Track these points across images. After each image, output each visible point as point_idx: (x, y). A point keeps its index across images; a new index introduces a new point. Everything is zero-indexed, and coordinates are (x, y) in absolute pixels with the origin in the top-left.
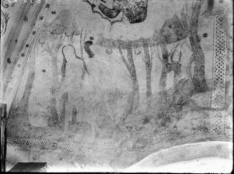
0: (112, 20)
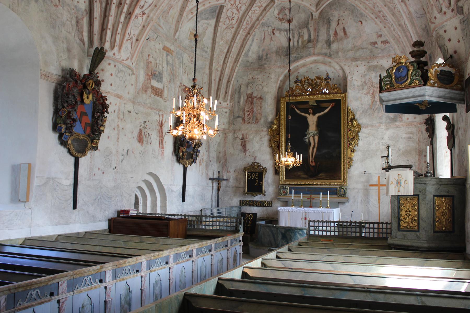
0: (282, 22)
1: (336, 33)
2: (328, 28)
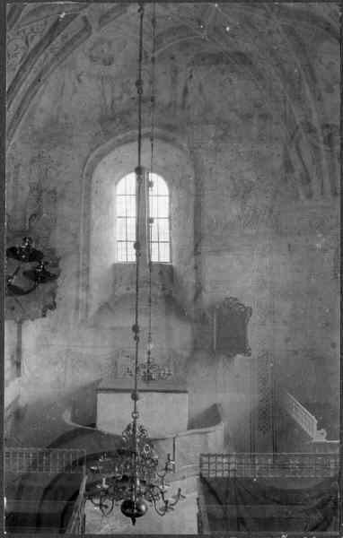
1: (186, 91)
2: (174, 81)
